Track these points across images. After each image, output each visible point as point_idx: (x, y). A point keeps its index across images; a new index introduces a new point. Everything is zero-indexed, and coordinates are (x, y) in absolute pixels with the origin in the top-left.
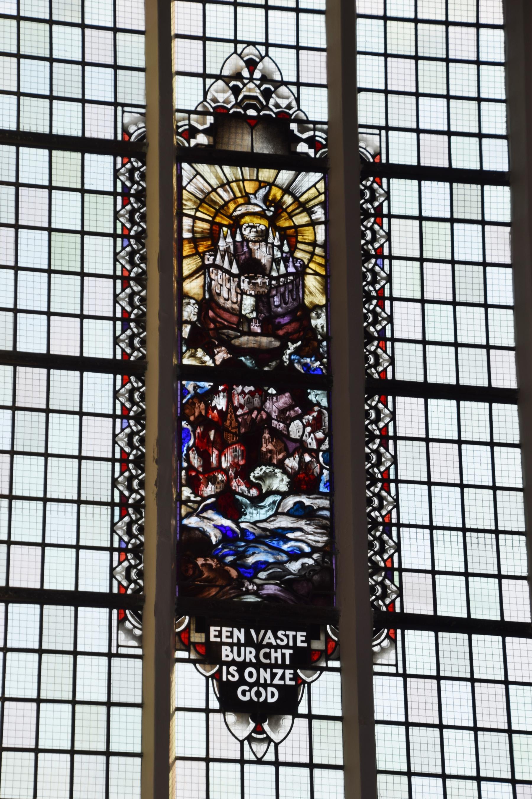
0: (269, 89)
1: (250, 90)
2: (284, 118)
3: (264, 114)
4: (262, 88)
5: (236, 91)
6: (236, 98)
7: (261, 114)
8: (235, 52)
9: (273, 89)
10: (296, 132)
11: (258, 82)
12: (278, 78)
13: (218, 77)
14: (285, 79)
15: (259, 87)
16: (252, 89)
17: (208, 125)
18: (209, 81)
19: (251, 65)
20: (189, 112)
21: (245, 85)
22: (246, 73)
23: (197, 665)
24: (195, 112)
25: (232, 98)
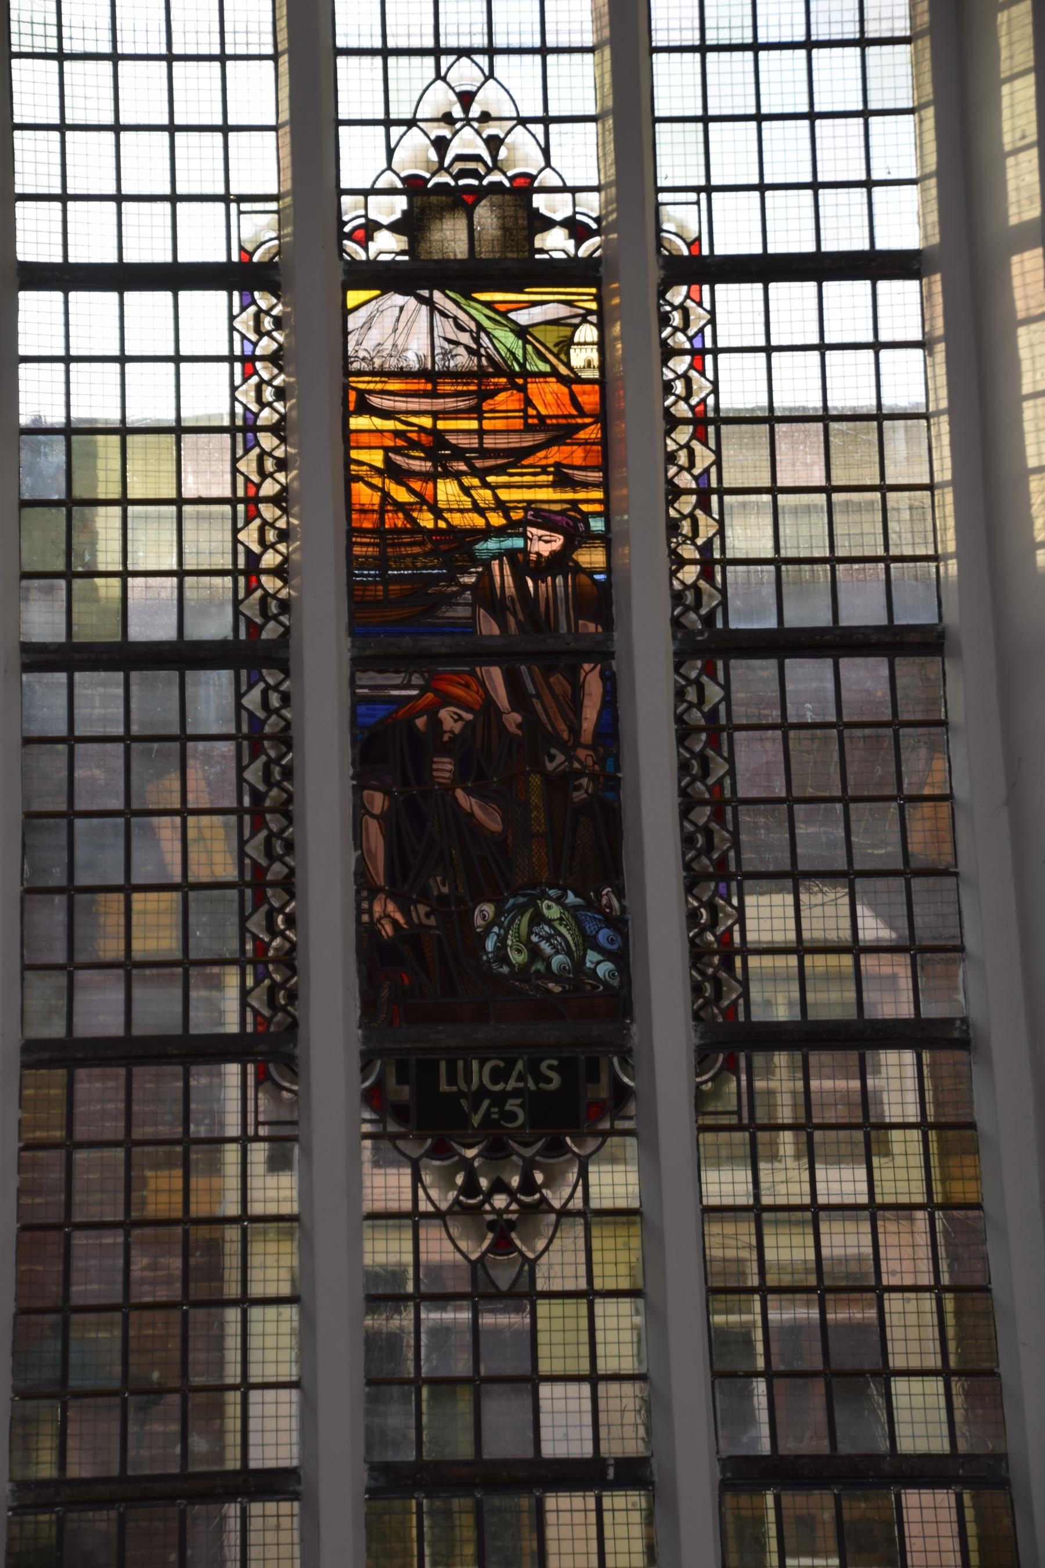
2: (524, 187)
3: (491, 184)
5: (441, 145)
7: (485, 182)
8: (439, 77)
9: (502, 136)
10: (542, 211)
12: (509, 111)
13: (411, 123)
15: (478, 133)
17: (398, 215)
18: (396, 131)
20: (366, 193)
21: (456, 133)
22: (457, 112)
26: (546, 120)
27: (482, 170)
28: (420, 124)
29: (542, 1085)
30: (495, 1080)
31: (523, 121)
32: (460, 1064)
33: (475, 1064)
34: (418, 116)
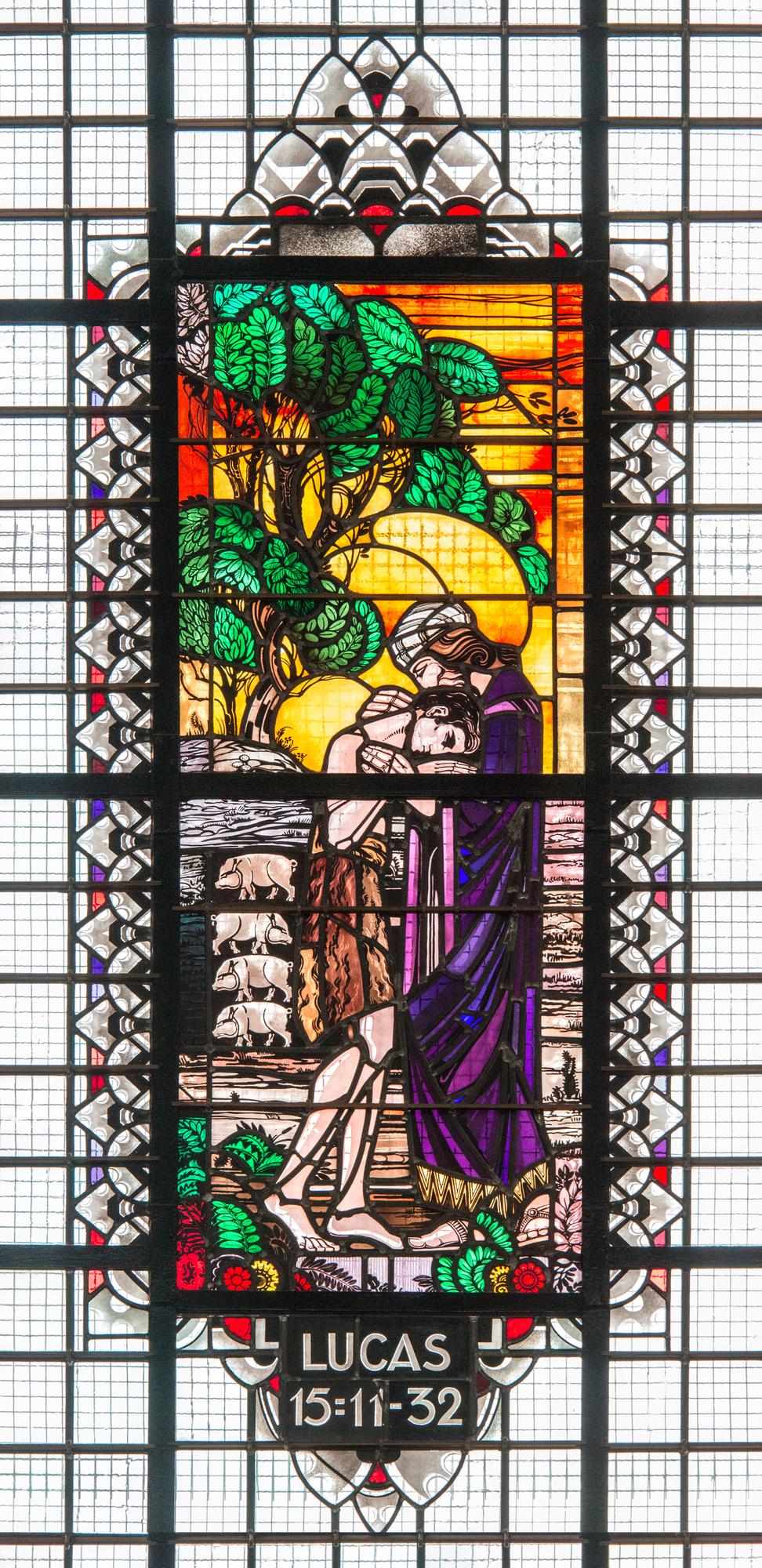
0: (426, 143)
1: (371, 153)
4: (407, 143)
5: (335, 155)
6: (337, 172)
9: (434, 143)
11: (395, 129)
12: (445, 108)
14: (471, 111)
15: (397, 140)
16: (377, 149)
18: (263, 138)
19: (377, 86)
21: (360, 140)
22: (360, 106)
23: (268, 1394)
24: (225, 219)
25: (324, 173)
26: (506, 124)
27: (399, 195)
28: (299, 127)
29: (428, 1365)
30: (374, 1360)
31: (470, 125)
32: (332, 1338)
33: (350, 1337)
34: (299, 115)
